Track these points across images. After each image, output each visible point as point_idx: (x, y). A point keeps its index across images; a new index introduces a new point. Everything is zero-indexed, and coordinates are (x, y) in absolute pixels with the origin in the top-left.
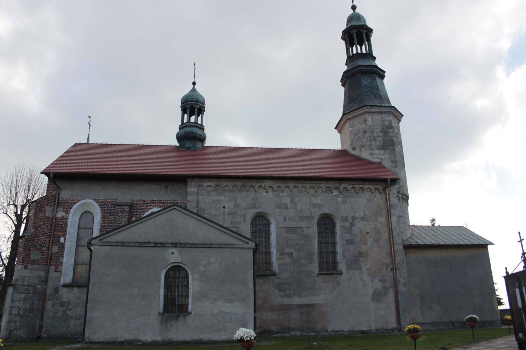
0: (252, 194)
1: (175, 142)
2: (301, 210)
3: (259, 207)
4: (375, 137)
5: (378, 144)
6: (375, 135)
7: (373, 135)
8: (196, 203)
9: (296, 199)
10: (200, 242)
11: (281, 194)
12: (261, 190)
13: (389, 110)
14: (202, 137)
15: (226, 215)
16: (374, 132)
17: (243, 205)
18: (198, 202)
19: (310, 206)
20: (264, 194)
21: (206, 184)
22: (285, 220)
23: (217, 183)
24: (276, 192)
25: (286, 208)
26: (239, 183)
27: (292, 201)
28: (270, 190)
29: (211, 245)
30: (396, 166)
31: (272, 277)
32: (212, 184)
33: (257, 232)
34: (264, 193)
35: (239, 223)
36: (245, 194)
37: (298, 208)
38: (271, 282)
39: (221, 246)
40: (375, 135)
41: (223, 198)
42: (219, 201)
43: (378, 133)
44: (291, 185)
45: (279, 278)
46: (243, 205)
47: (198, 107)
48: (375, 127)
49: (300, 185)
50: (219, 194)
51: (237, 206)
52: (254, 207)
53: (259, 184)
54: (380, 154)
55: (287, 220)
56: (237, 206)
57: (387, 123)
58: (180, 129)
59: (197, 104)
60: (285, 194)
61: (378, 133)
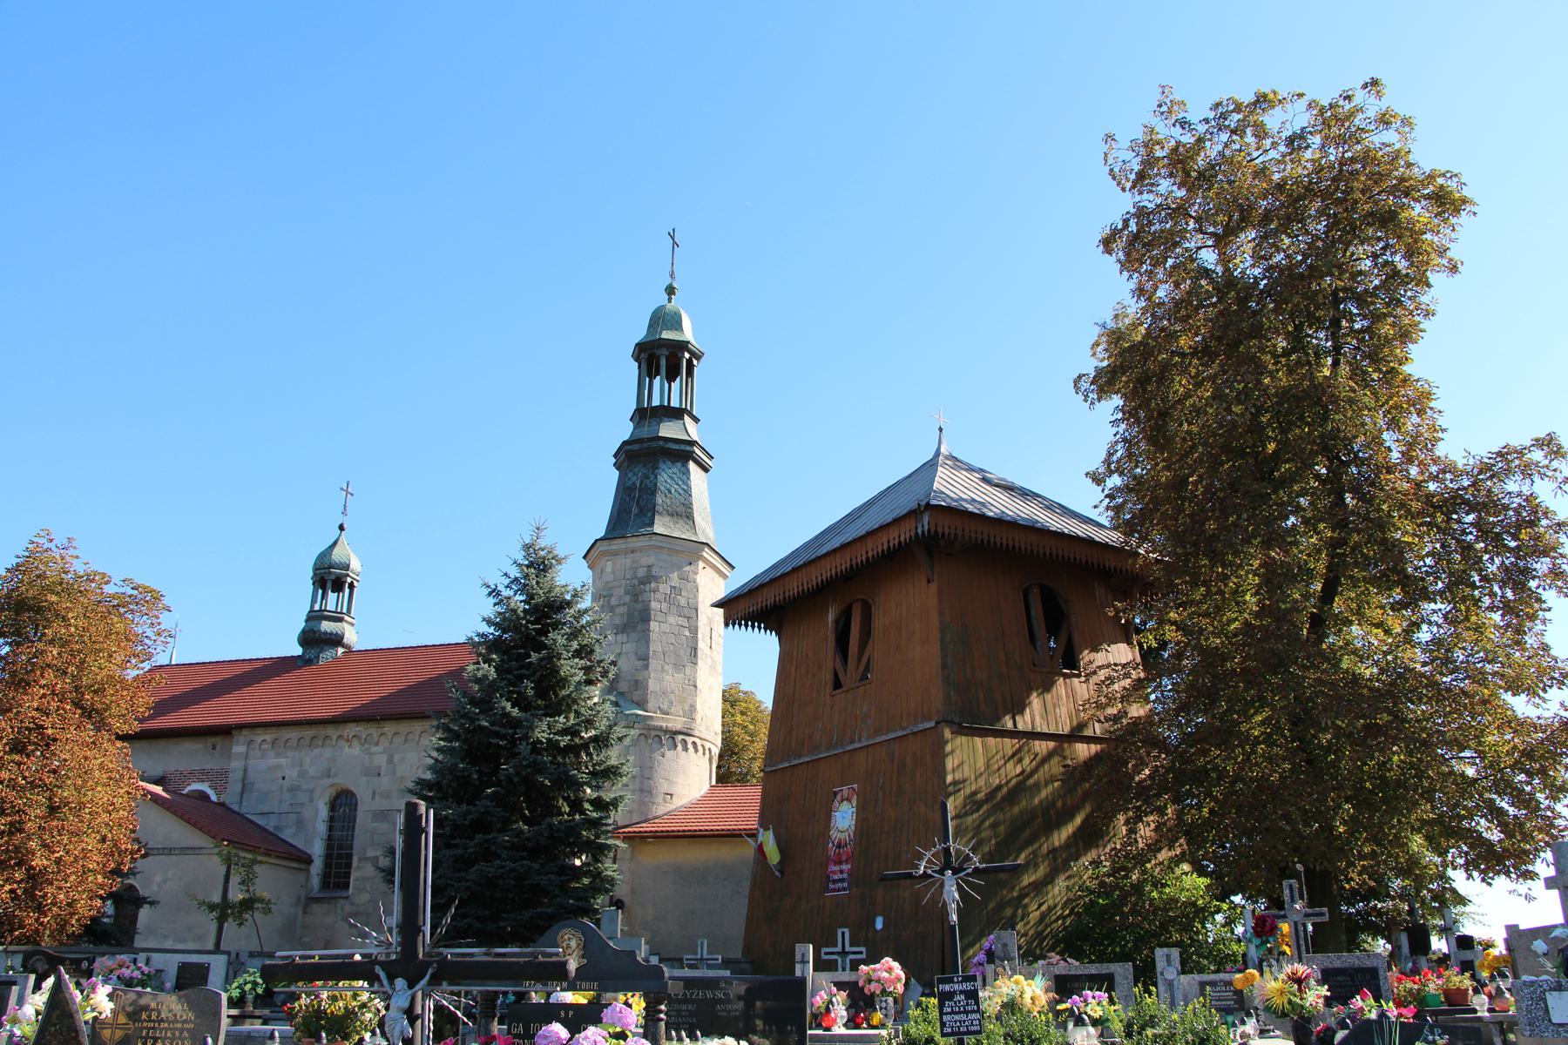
0: (327, 752)
1: (298, 651)
2: (402, 777)
3: (336, 775)
4: (612, 607)
5: (617, 621)
6: (614, 601)
7: (609, 601)
8: (242, 772)
9: (397, 757)
10: (160, 846)
11: (374, 749)
12: (342, 743)
13: (648, 543)
14: (333, 637)
15: (285, 790)
16: (611, 595)
17: (312, 772)
18: (245, 770)
19: (417, 769)
20: (347, 750)
21: (259, 739)
22: (373, 798)
23: (275, 736)
24: (366, 746)
25: (379, 774)
26: (309, 732)
27: (390, 761)
28: (355, 742)
29: (171, 849)
30: (646, 667)
31: (342, 901)
32: (268, 738)
33: (347, 819)
34: (347, 747)
35: (303, 804)
36: (317, 751)
37: (399, 774)
38: (339, 911)
39: (185, 851)
40: (614, 601)
41: (282, 761)
42: (278, 767)
43: (620, 597)
44: (389, 728)
45: (353, 904)
46: (312, 772)
47: (333, 577)
48: (617, 584)
49: (404, 727)
50: (278, 755)
51: (302, 774)
52: (329, 776)
53: (338, 733)
54: (616, 643)
55: (377, 798)
56: (302, 774)
57: (641, 573)
58: (307, 621)
59: (330, 573)
60: (379, 749)
61: (620, 597)
